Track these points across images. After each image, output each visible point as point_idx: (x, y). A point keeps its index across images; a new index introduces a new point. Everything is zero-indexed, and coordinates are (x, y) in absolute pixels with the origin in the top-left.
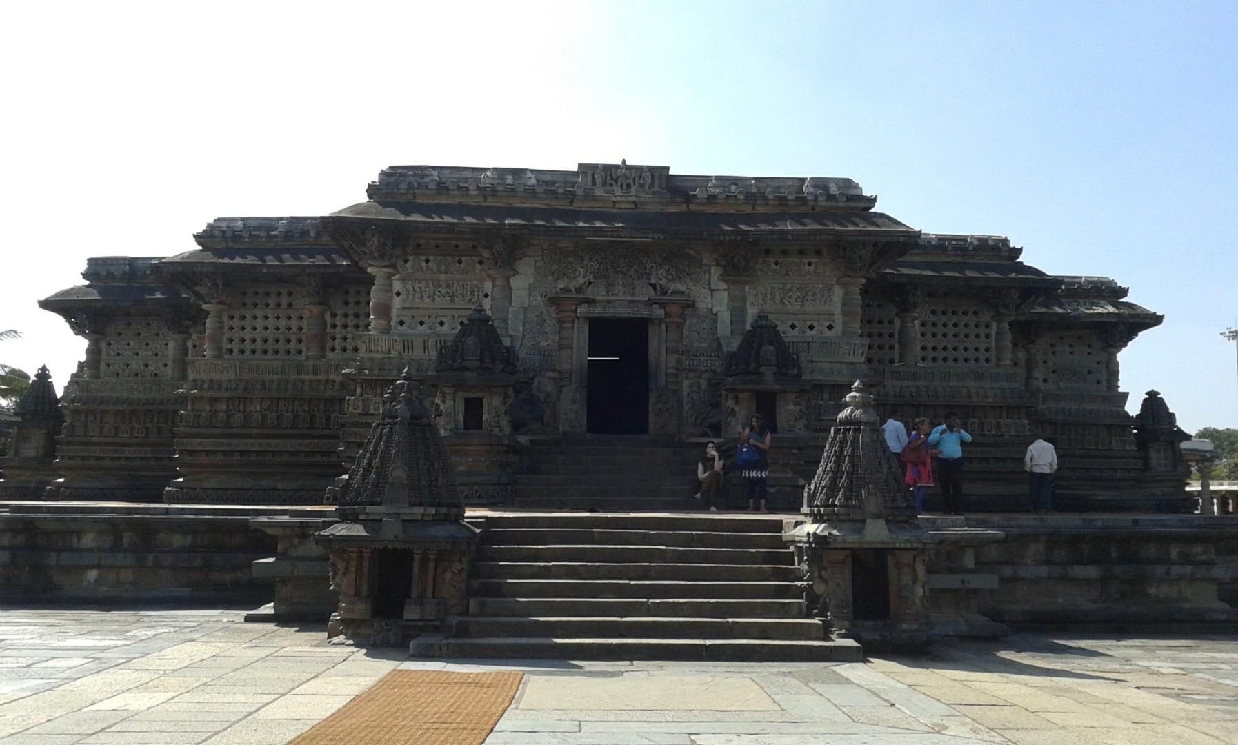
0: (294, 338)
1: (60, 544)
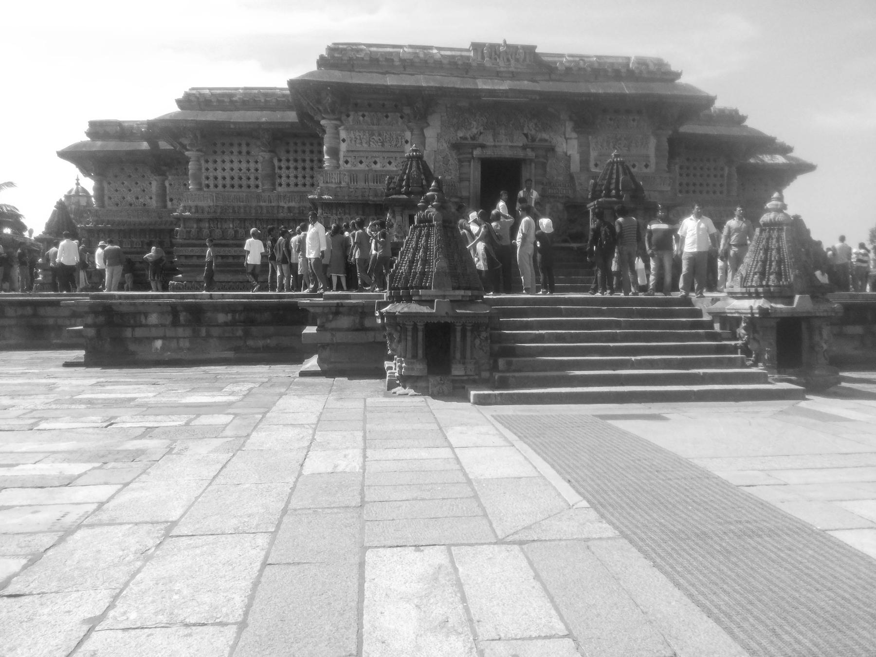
0: (252, 177)
1: (132, 322)
